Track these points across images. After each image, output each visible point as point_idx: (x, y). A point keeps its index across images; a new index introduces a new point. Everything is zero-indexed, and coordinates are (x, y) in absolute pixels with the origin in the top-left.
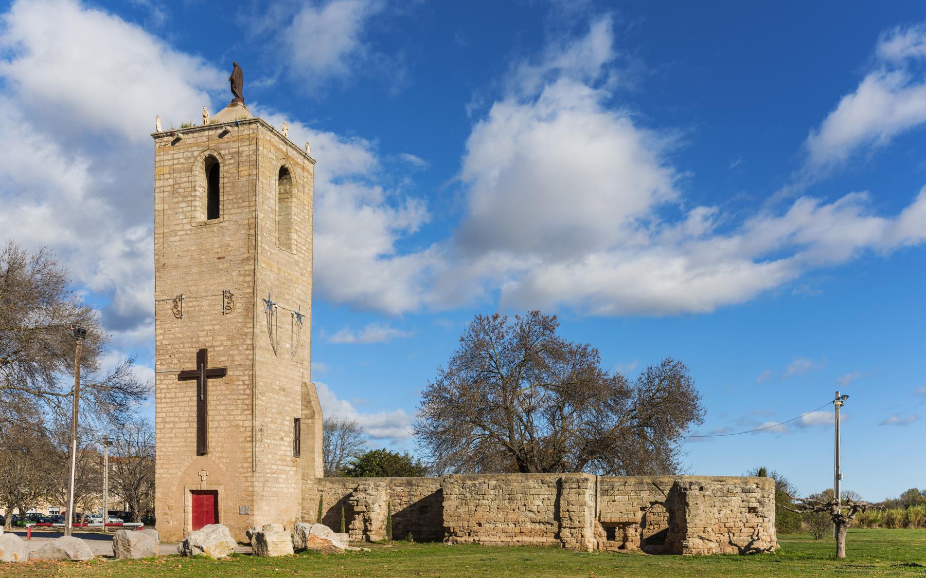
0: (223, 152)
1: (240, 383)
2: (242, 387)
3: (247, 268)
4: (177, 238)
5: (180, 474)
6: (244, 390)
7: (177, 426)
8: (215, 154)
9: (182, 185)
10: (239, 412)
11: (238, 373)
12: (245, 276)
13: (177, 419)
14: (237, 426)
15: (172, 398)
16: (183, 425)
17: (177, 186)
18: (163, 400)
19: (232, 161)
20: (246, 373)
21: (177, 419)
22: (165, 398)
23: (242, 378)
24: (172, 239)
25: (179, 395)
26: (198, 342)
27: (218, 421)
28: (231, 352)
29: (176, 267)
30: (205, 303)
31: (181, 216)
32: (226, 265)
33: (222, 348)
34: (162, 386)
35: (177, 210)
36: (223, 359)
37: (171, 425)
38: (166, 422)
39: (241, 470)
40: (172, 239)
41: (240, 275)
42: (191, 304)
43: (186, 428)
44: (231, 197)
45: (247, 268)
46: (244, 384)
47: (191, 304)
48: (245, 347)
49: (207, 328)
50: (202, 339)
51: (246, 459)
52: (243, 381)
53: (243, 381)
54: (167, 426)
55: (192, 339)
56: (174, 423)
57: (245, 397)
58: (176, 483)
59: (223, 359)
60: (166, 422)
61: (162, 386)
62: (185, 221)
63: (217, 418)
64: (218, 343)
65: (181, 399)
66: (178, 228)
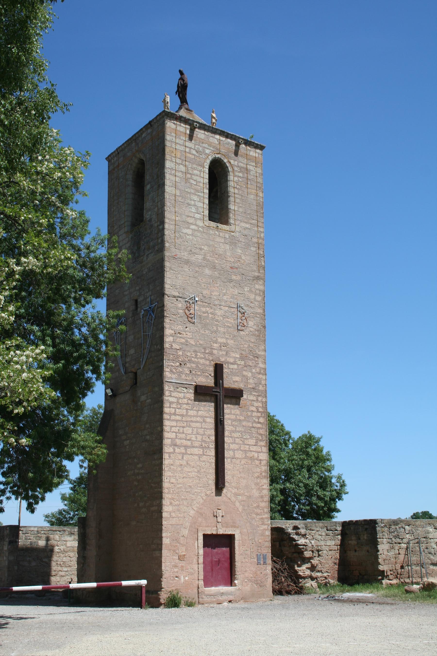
0: (232, 162)
1: (254, 409)
2: (255, 414)
3: (257, 286)
4: (189, 232)
5: (192, 513)
6: (259, 418)
7: (189, 451)
8: (225, 161)
9: (195, 178)
10: (252, 442)
11: (252, 398)
12: (256, 295)
13: (189, 443)
14: (252, 459)
15: (182, 416)
16: (196, 451)
17: (189, 176)
18: (173, 417)
19: (241, 175)
20: (260, 399)
21: (189, 443)
22: (175, 414)
23: (256, 404)
24: (185, 231)
25: (191, 413)
26: (211, 354)
27: (234, 450)
28: (245, 373)
29: (187, 262)
30: (219, 312)
31: (193, 210)
32: (238, 278)
33: (235, 366)
34: (171, 399)
35: (189, 201)
36: (237, 379)
37: (183, 450)
38: (175, 445)
39: (259, 511)
40: (185, 231)
41: (251, 291)
42: (204, 309)
43: (200, 456)
44: (241, 210)
45: (257, 286)
46: (258, 411)
47: (204, 309)
48: (258, 370)
49: (220, 340)
50: (215, 352)
51: (262, 497)
52: (257, 408)
53: (257, 408)
54: (177, 450)
55: (205, 349)
56: (186, 447)
57: (259, 425)
58: (188, 524)
59: (237, 379)
60: (175, 445)
61: (171, 399)
62: (197, 216)
63: (232, 446)
64: (232, 360)
65: (194, 419)
66: (191, 220)
